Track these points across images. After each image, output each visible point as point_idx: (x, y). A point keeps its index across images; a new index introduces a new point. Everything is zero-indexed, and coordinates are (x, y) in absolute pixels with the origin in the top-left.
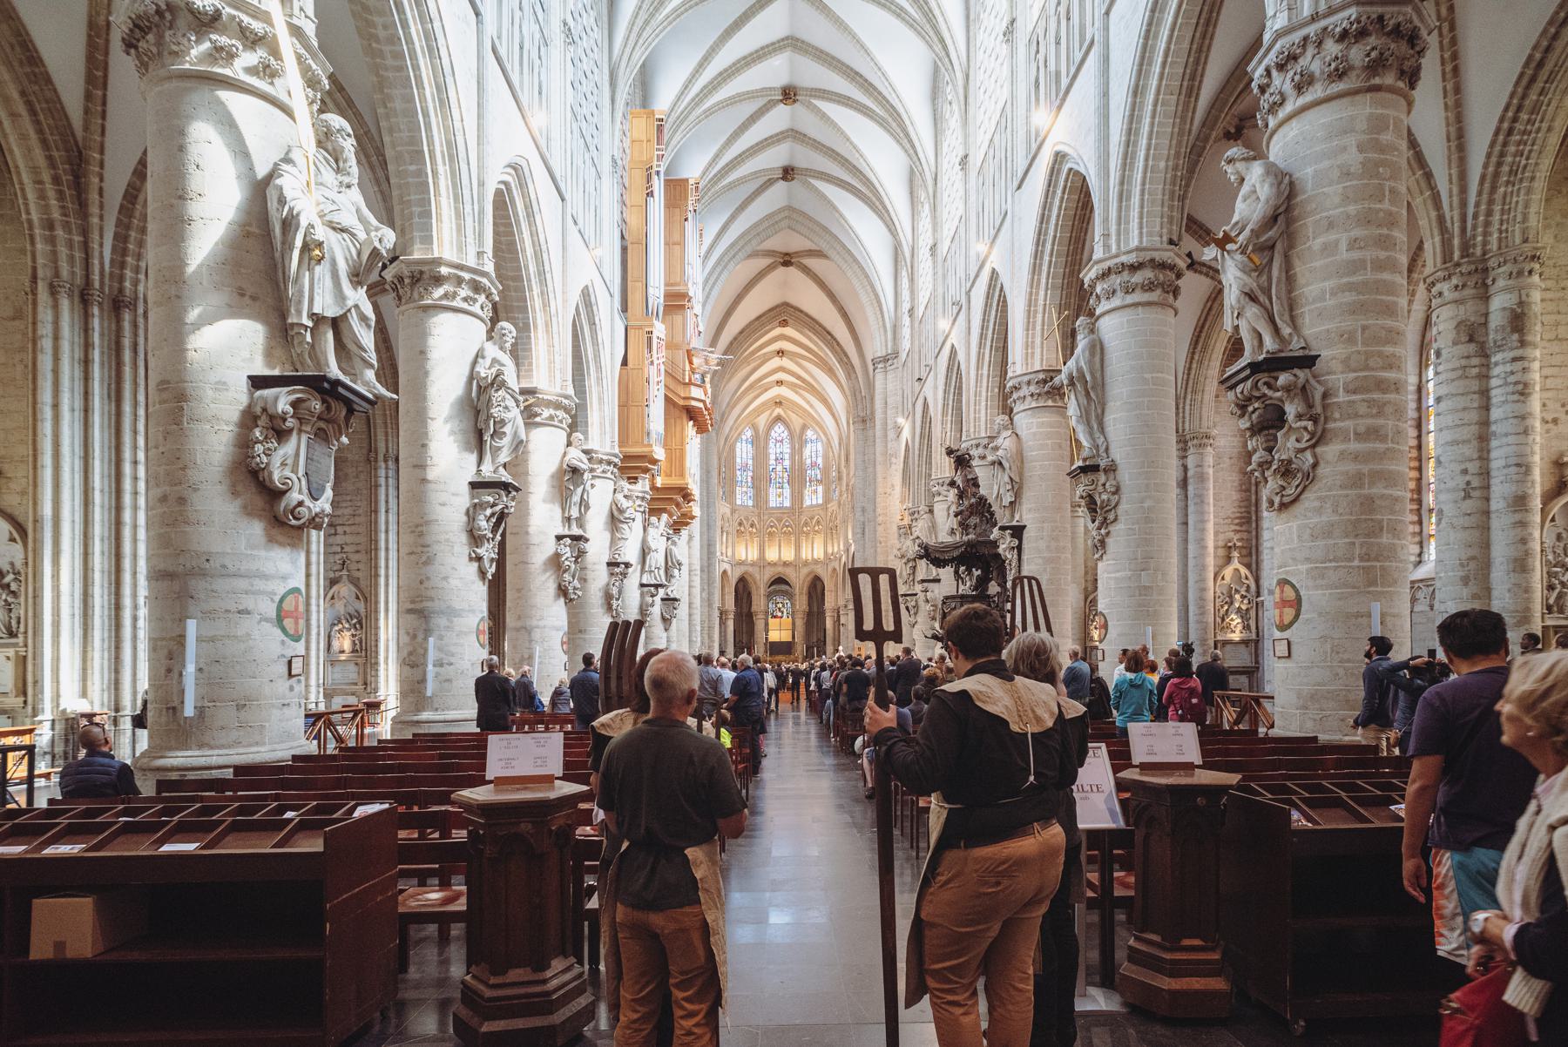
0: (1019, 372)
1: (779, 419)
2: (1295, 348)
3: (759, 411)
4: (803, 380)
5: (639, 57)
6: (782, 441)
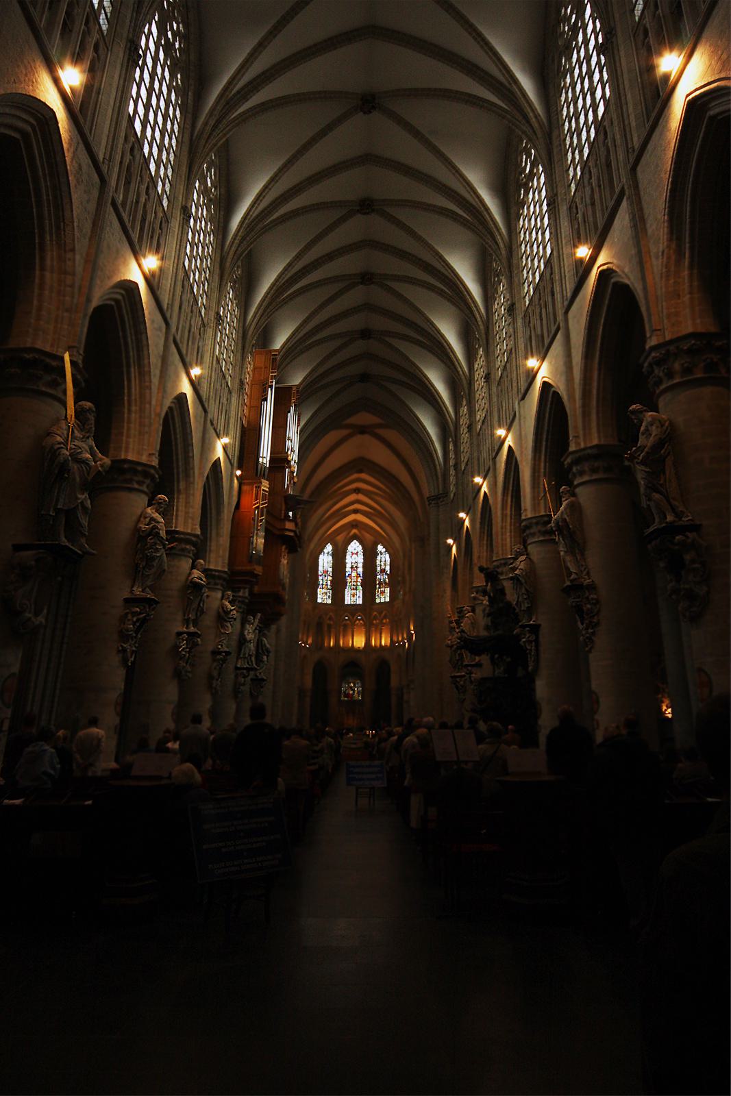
3: (338, 532)
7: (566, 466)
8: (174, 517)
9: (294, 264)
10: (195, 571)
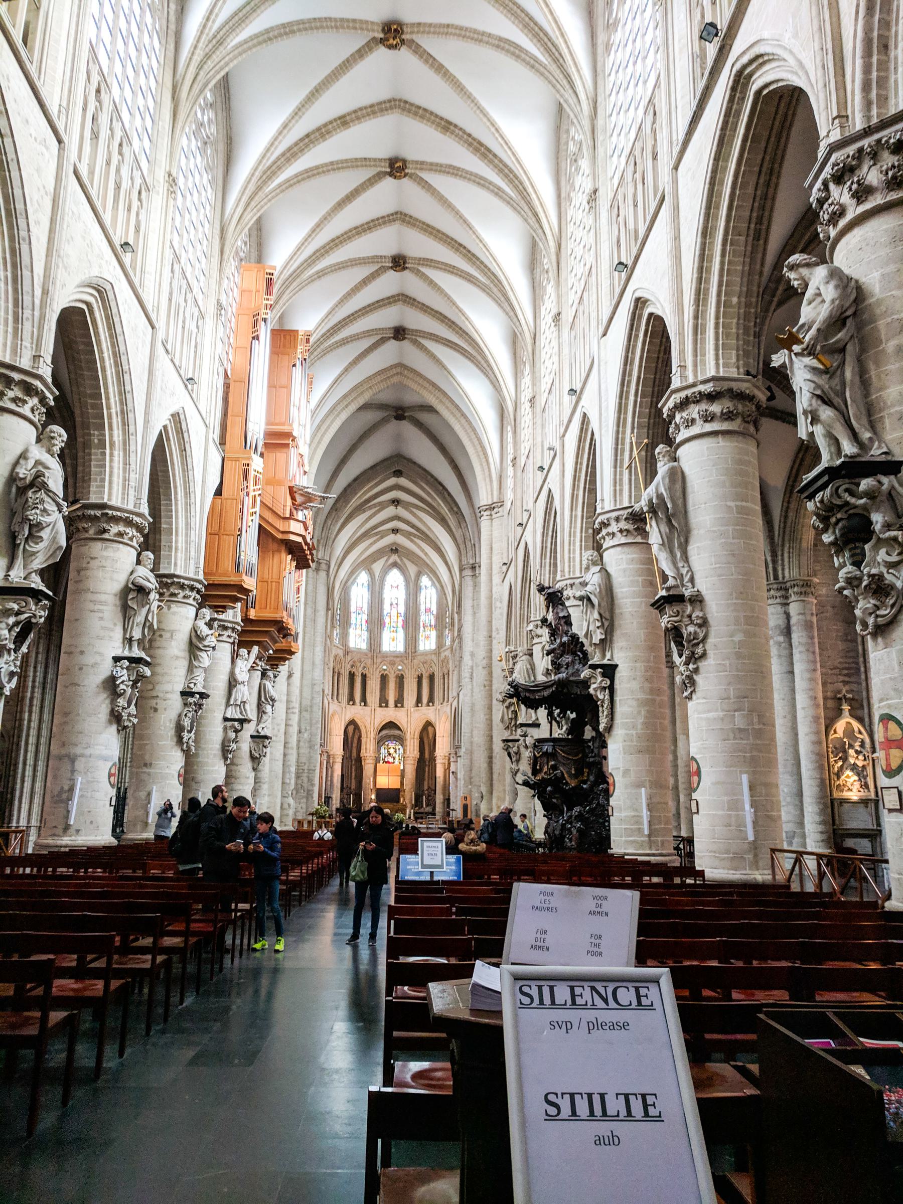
0: (607, 509)
1: (395, 565)
2: (876, 452)
4: (418, 529)
5: (250, 219)
6: (397, 587)
7: (665, 416)
8: (107, 484)
9: (291, 125)
10: (140, 568)
